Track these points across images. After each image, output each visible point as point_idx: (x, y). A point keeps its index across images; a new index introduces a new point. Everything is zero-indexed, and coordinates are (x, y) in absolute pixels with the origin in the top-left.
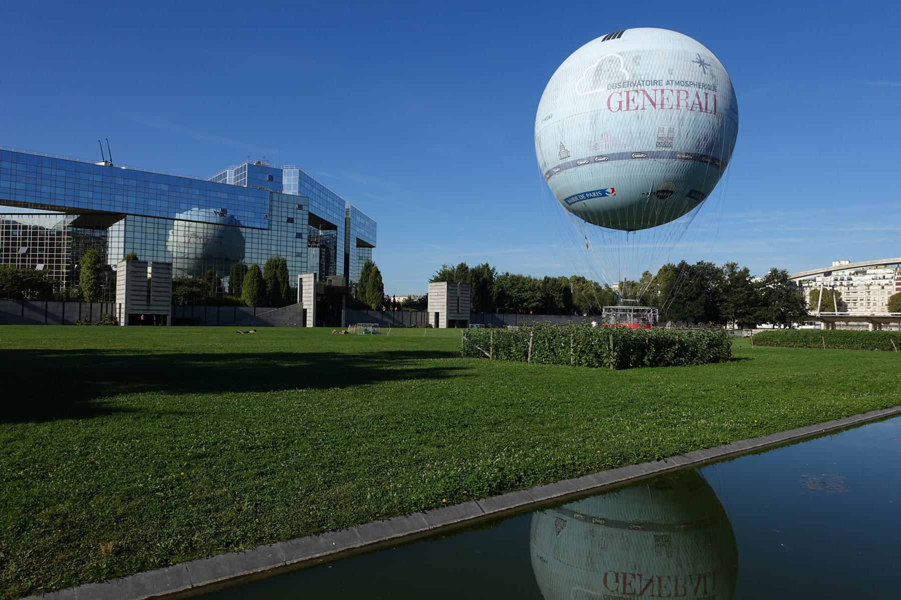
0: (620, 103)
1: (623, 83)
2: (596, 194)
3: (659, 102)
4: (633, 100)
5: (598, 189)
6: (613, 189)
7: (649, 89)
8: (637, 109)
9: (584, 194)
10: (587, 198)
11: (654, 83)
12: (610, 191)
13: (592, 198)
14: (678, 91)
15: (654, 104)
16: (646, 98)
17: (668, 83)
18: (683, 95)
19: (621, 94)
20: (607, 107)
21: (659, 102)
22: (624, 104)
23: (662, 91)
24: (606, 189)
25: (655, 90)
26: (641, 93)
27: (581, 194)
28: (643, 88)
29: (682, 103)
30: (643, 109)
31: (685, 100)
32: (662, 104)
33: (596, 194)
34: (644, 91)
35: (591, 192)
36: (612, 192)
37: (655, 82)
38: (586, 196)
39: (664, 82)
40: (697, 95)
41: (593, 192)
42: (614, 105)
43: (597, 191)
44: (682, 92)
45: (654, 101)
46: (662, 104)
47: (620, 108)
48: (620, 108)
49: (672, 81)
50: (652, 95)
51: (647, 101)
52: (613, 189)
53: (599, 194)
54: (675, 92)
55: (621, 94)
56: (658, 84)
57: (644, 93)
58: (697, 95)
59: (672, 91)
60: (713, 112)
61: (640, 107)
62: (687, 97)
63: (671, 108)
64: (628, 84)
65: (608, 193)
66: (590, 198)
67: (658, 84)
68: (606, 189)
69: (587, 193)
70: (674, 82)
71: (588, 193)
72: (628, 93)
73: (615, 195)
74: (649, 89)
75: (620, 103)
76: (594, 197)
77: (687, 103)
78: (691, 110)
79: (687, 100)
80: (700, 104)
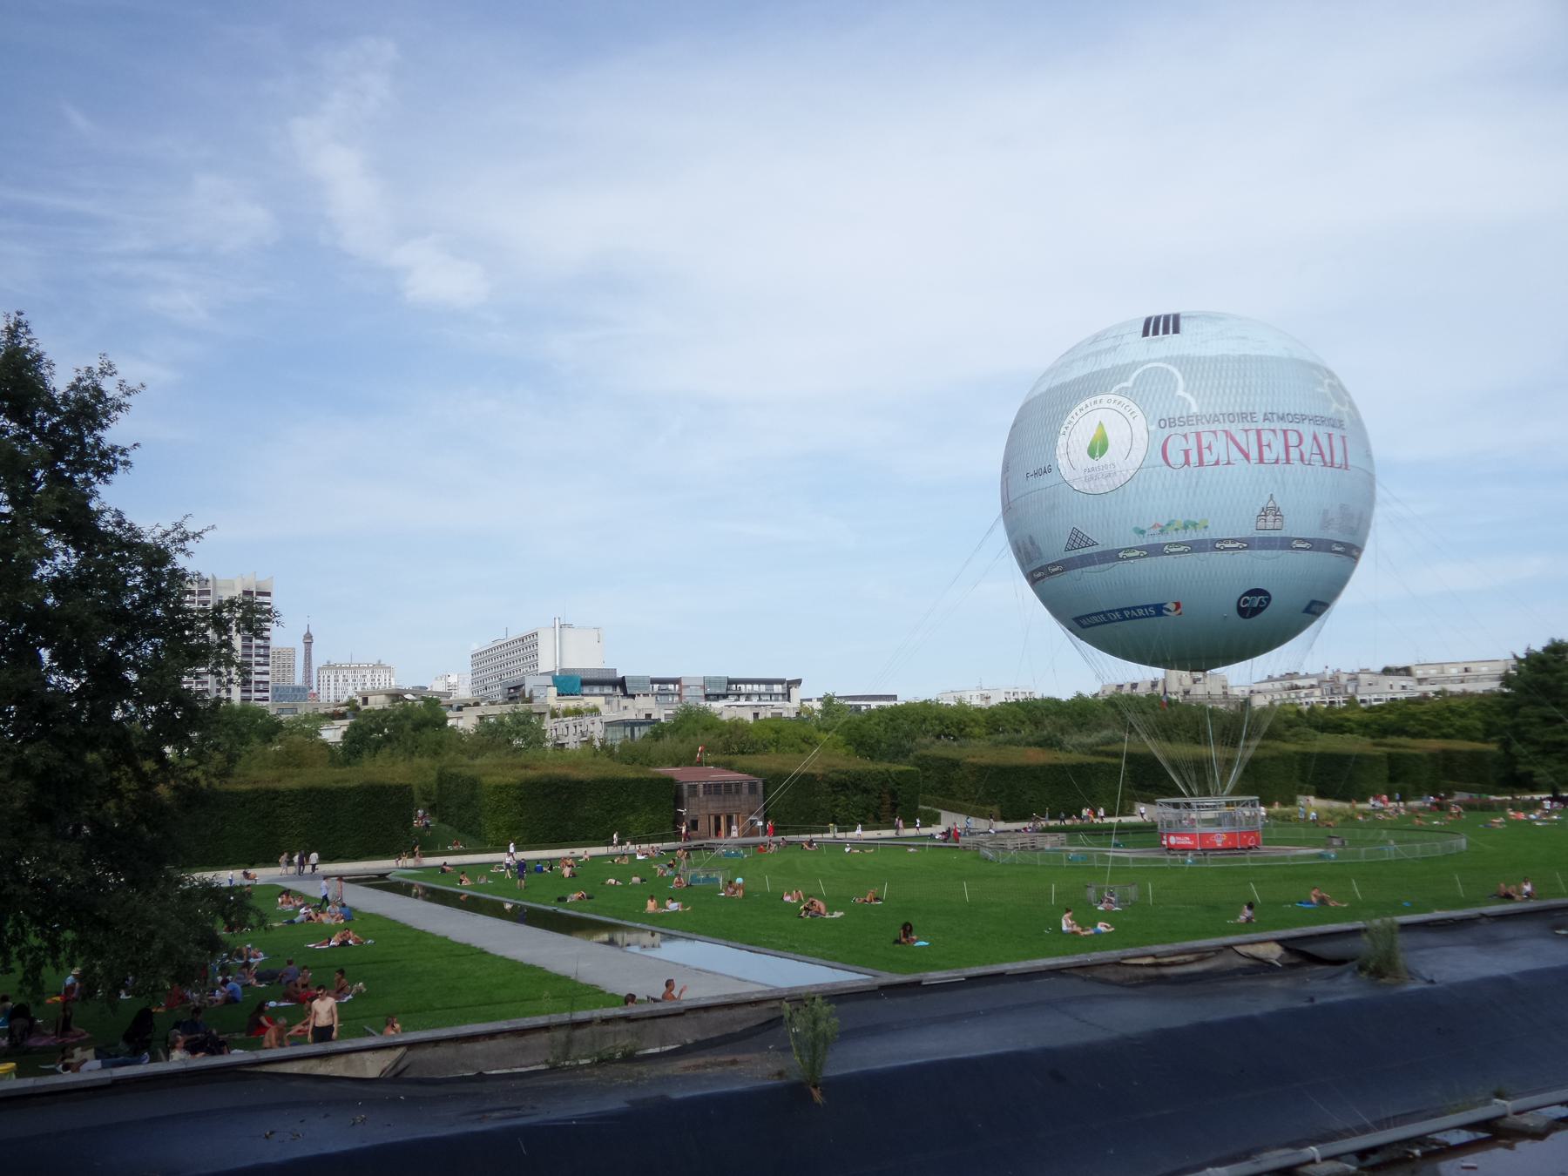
0: (1187, 453)
1: (1188, 417)
2: (1144, 612)
3: (1254, 454)
4: (1209, 448)
5: (1151, 603)
6: (1178, 605)
7: (1236, 429)
8: (1217, 463)
9: (1121, 611)
10: (1125, 619)
11: (1243, 418)
12: (1172, 606)
13: (1135, 618)
14: (1285, 432)
15: (1247, 456)
18: (1293, 439)
19: (1185, 436)
20: (1163, 462)
22: (1194, 458)
23: (1259, 432)
24: (1165, 604)
26: (1222, 436)
27: (1113, 611)
28: (1227, 426)
29: (1294, 453)
30: (1229, 463)
33: (1144, 612)
34: (1226, 432)
35: (1134, 608)
36: (1176, 609)
37: (1243, 417)
38: (1123, 615)
40: (1315, 438)
41: (1138, 607)
42: (1176, 457)
43: (1147, 607)
44: (1289, 433)
45: (1247, 451)
47: (1187, 462)
48: (1187, 462)
49: (1272, 414)
50: (1241, 438)
51: (1236, 454)
52: (1178, 605)
53: (1150, 612)
54: (1280, 435)
55: (1185, 436)
56: (1249, 418)
57: (1227, 436)
58: (1315, 438)
59: (1274, 431)
60: (1344, 467)
61: (1224, 459)
63: (1277, 462)
64: (1197, 420)
65: (1169, 610)
66: (1131, 618)
67: (1249, 418)
68: (1165, 604)
69: (1126, 609)
70: (1275, 417)
71: (1129, 609)
72: (1198, 435)
73: (1180, 614)
74: (1236, 429)
75: (1187, 453)
76: (1139, 617)
80: (1322, 454)
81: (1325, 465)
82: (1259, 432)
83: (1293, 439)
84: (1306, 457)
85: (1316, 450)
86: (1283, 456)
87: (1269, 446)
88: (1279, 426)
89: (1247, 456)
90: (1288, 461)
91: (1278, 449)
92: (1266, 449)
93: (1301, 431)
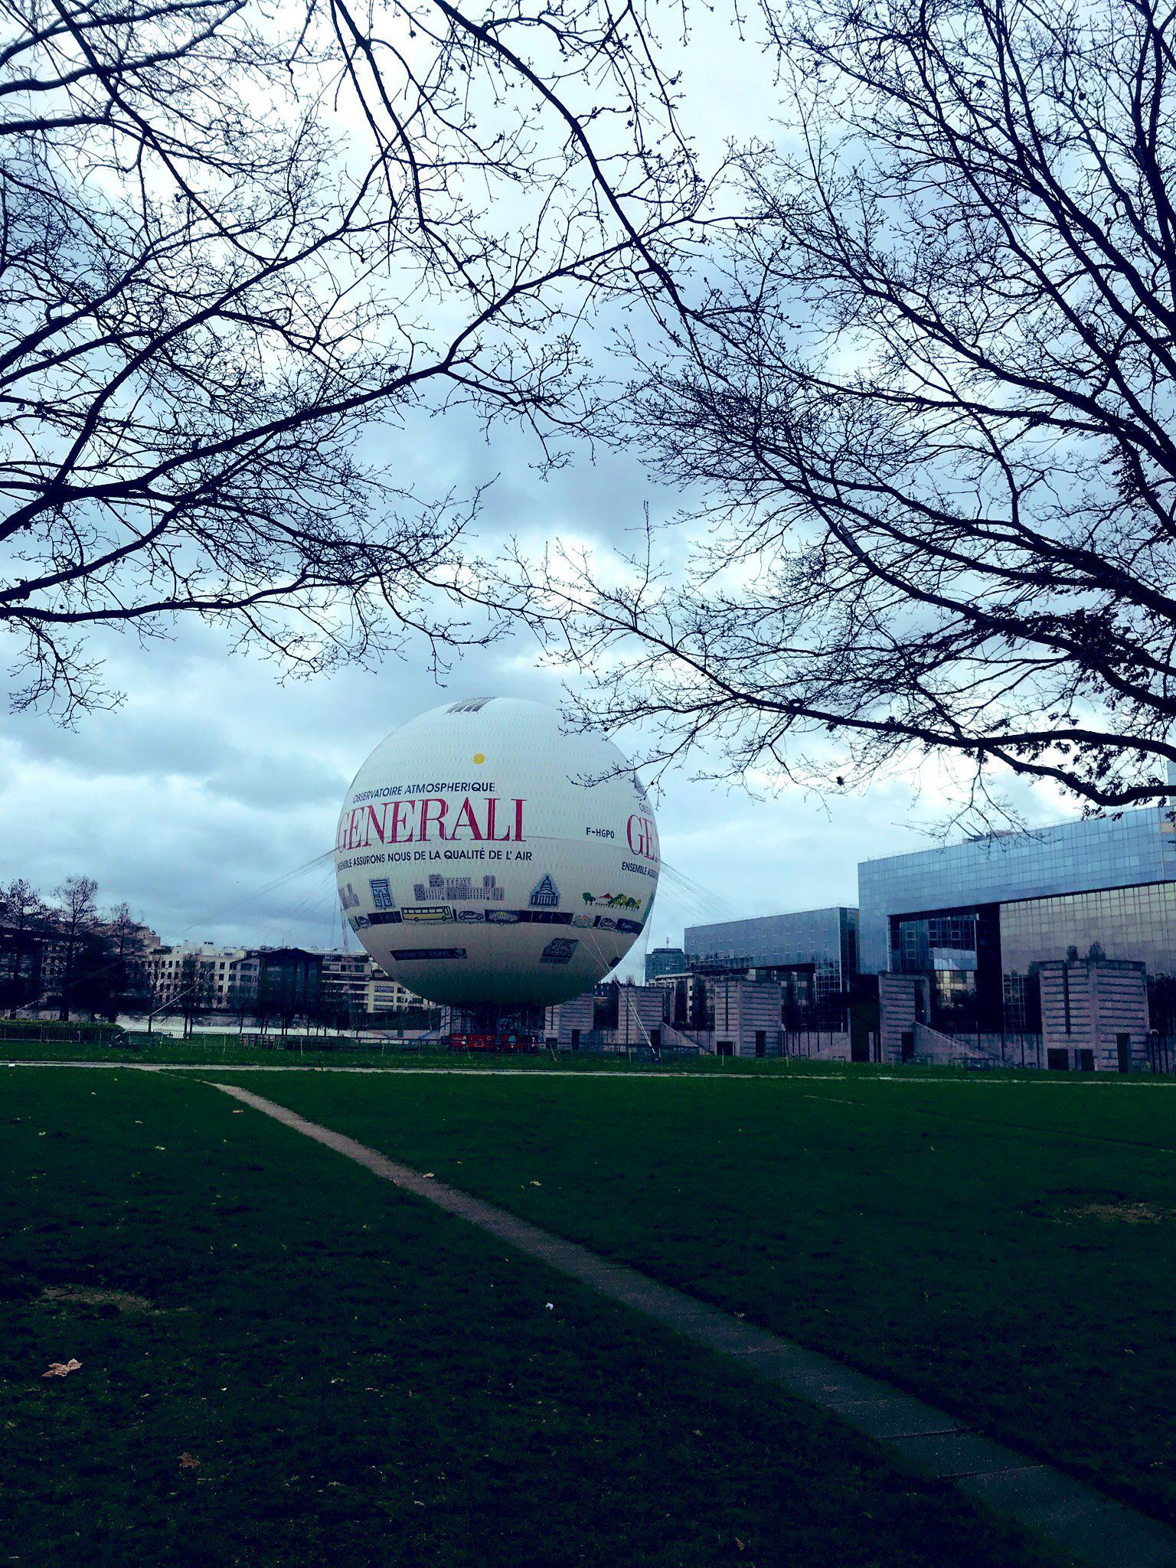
3: (388, 833)
4: (356, 827)
15: (381, 833)
18: (434, 809)
21: (388, 833)
25: (385, 805)
26: (367, 810)
29: (433, 828)
30: (367, 844)
31: (438, 819)
32: (394, 836)
39: (404, 789)
40: (466, 803)
46: (394, 836)
51: (374, 834)
54: (419, 806)
58: (466, 803)
59: (413, 803)
60: (513, 833)
61: (363, 843)
62: (443, 814)
63: (410, 840)
77: (442, 824)
78: (453, 838)
81: (478, 836)
82: (397, 805)
83: (434, 809)
84: (449, 832)
85: (465, 820)
86: (417, 833)
87: (404, 821)
89: (381, 833)
90: (423, 837)
91: (414, 820)
92: (400, 825)
93: (448, 802)
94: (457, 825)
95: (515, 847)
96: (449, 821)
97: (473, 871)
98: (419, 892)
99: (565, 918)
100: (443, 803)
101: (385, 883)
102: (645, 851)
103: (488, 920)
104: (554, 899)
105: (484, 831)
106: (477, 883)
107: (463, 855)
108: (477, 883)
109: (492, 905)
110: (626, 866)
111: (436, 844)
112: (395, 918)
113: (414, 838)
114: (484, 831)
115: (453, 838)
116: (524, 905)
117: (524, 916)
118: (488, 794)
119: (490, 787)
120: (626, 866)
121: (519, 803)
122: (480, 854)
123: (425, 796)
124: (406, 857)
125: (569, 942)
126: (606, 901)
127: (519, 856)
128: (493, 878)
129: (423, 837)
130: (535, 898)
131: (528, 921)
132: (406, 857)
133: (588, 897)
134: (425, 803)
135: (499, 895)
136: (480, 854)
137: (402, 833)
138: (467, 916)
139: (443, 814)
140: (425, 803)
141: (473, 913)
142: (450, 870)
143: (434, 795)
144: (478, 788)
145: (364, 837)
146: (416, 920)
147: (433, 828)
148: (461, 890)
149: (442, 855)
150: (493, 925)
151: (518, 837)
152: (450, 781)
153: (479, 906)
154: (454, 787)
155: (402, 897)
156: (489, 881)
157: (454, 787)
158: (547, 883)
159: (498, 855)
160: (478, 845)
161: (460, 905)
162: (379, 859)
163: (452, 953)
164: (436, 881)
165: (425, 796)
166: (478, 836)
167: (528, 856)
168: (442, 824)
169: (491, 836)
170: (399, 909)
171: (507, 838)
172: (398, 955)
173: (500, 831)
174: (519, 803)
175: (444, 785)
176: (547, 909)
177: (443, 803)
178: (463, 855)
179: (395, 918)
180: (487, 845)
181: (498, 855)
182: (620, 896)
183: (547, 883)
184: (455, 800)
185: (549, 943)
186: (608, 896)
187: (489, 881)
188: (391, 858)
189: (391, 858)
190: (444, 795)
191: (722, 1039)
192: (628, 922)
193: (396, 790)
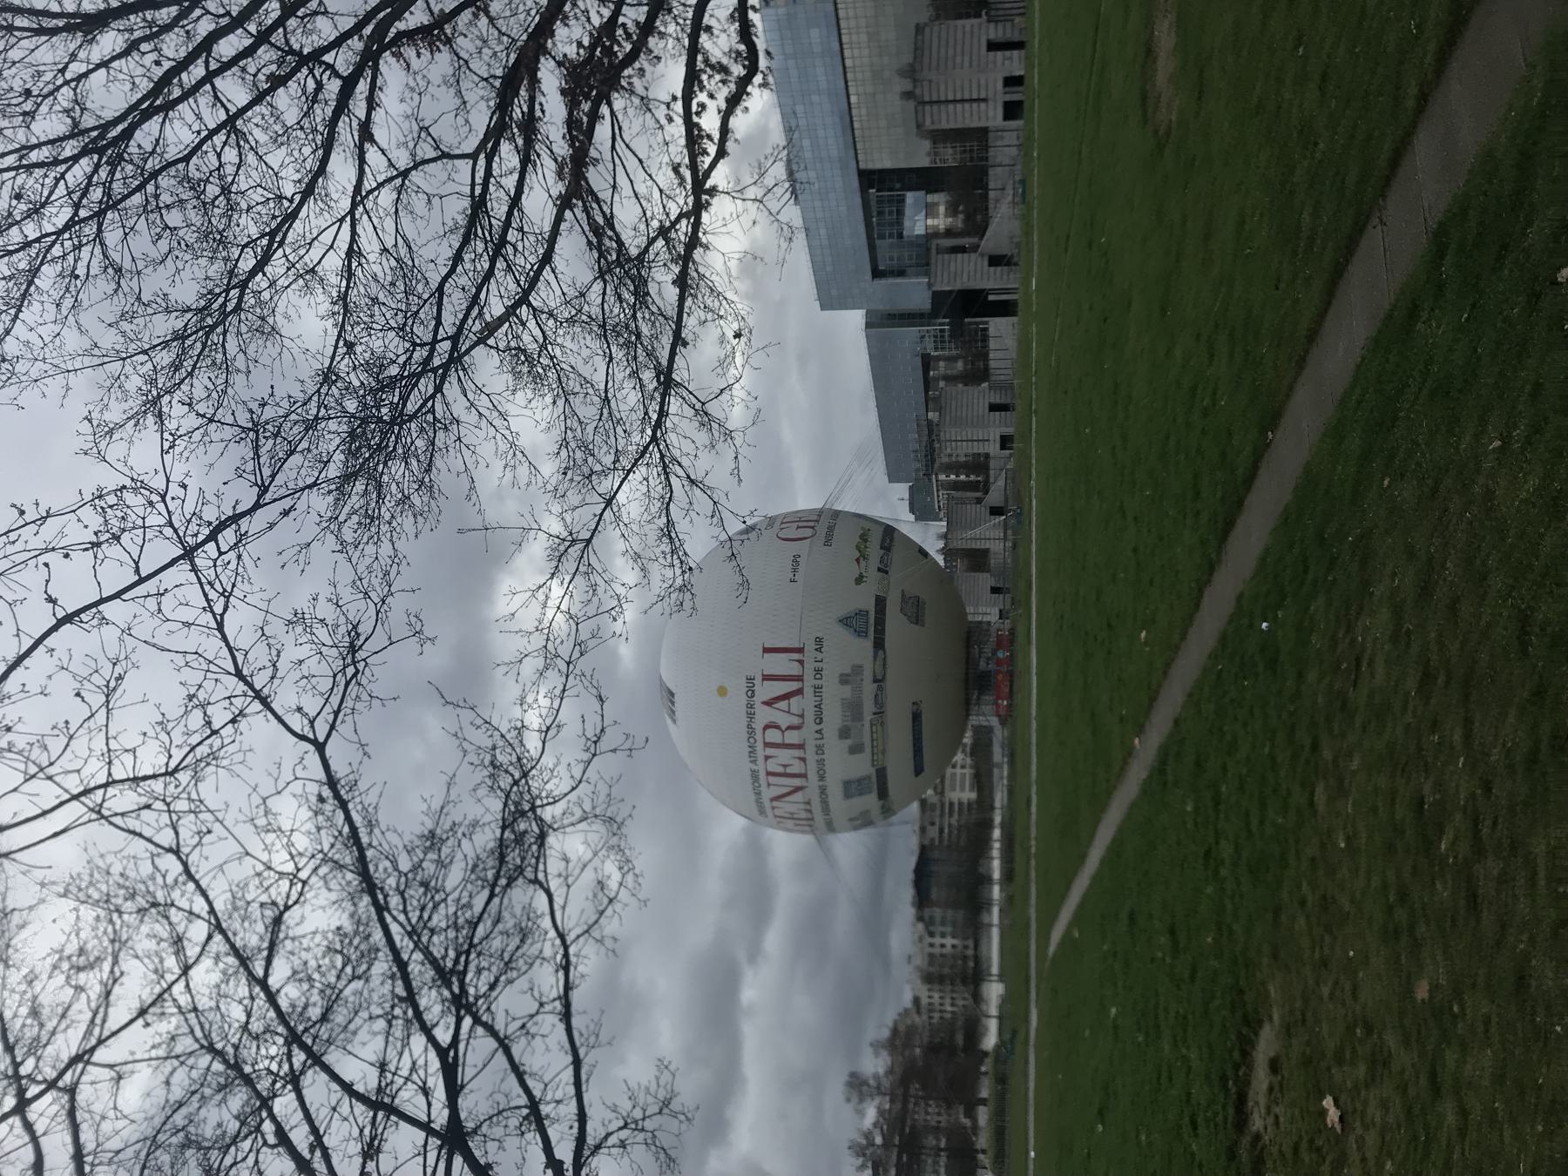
3: (797, 782)
15: (798, 789)
16: (787, 799)
17: (754, 762)
18: (774, 736)
21: (797, 782)
25: (769, 785)
26: (775, 804)
29: (792, 737)
40: (769, 703)
51: (798, 796)
54: (769, 751)
58: (769, 703)
59: (767, 758)
60: (796, 656)
62: (777, 727)
63: (803, 760)
77: (789, 728)
78: (802, 716)
79: (783, 728)
80: (787, 697)
81: (799, 692)
82: (769, 774)
83: (774, 736)
84: (796, 721)
85: (783, 705)
86: (796, 753)
87: (785, 766)
88: (760, 751)
89: (798, 789)
90: (801, 746)
91: (785, 756)
92: (789, 770)
93: (766, 722)
94: (789, 712)
95: (810, 654)
96: (784, 720)
97: (834, 695)
98: (856, 749)
99: (880, 602)
100: (766, 727)
101: (847, 785)
102: (812, 524)
103: (883, 680)
104: (861, 614)
105: (794, 686)
106: (847, 691)
107: (818, 706)
108: (847, 691)
109: (868, 675)
110: (828, 543)
111: (808, 734)
112: (881, 774)
113: (802, 755)
114: (794, 686)
115: (802, 716)
116: (868, 644)
117: (879, 644)
118: (758, 681)
119: (750, 679)
120: (828, 543)
121: (766, 650)
122: (817, 689)
123: (759, 746)
124: (821, 763)
125: (904, 598)
126: (863, 563)
127: (819, 650)
128: (841, 675)
129: (801, 746)
130: (861, 633)
131: (883, 640)
132: (821, 763)
133: (859, 580)
134: (767, 745)
135: (858, 669)
136: (817, 689)
137: (797, 768)
138: (879, 700)
139: (777, 727)
140: (767, 745)
141: (876, 696)
142: (834, 717)
143: (759, 736)
144: (751, 693)
145: (802, 806)
146: (884, 752)
147: (792, 737)
148: (853, 709)
149: (819, 727)
150: (888, 676)
151: (800, 650)
152: (744, 721)
153: (869, 688)
154: (751, 716)
155: (862, 766)
156: (844, 680)
157: (751, 716)
158: (845, 621)
159: (818, 671)
160: (809, 691)
161: (869, 708)
162: (823, 790)
163: (916, 717)
164: (844, 733)
165: (759, 746)
166: (799, 692)
167: (819, 641)
168: (789, 728)
169: (799, 678)
170: (872, 771)
171: (801, 662)
172: (918, 770)
173: (795, 669)
174: (766, 650)
175: (749, 726)
176: (872, 621)
177: (766, 727)
178: (818, 706)
179: (881, 774)
180: (809, 681)
181: (818, 671)
182: (858, 548)
183: (845, 621)
184: (764, 715)
185: (905, 618)
186: (858, 560)
187: (844, 680)
188: (822, 778)
189: (822, 778)
190: (758, 726)
191: (998, 445)
192: (883, 541)
193: (754, 775)
